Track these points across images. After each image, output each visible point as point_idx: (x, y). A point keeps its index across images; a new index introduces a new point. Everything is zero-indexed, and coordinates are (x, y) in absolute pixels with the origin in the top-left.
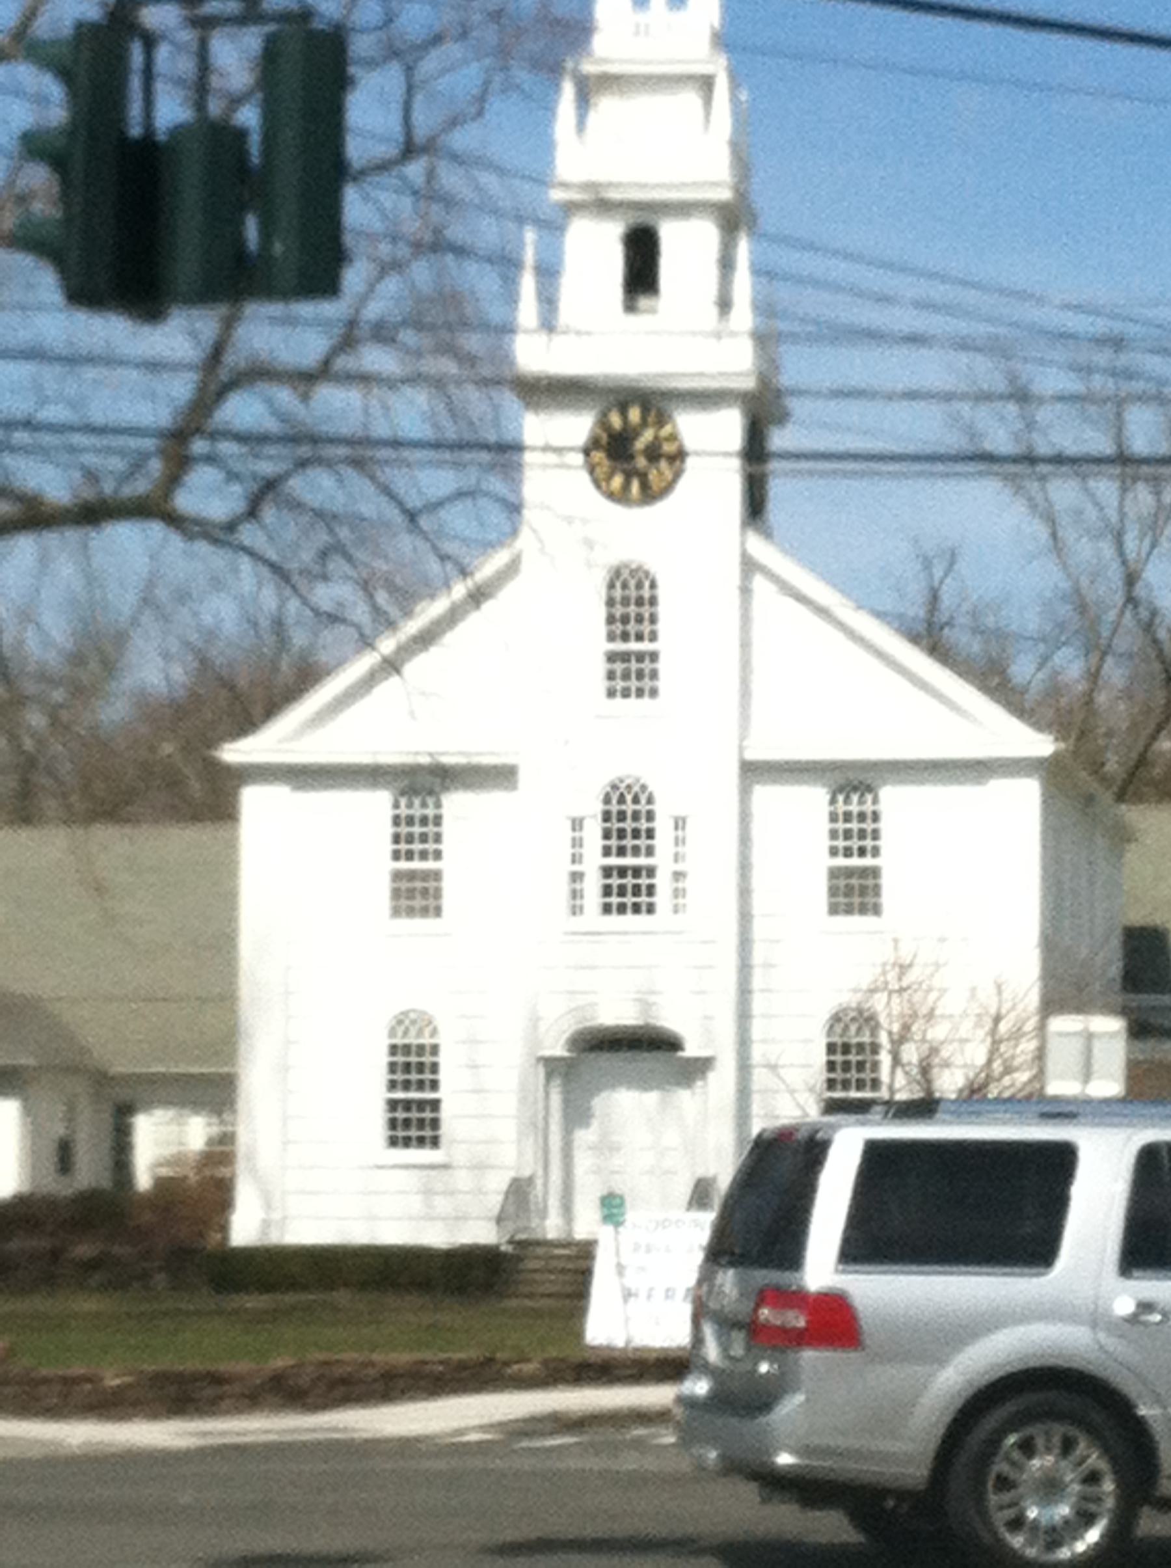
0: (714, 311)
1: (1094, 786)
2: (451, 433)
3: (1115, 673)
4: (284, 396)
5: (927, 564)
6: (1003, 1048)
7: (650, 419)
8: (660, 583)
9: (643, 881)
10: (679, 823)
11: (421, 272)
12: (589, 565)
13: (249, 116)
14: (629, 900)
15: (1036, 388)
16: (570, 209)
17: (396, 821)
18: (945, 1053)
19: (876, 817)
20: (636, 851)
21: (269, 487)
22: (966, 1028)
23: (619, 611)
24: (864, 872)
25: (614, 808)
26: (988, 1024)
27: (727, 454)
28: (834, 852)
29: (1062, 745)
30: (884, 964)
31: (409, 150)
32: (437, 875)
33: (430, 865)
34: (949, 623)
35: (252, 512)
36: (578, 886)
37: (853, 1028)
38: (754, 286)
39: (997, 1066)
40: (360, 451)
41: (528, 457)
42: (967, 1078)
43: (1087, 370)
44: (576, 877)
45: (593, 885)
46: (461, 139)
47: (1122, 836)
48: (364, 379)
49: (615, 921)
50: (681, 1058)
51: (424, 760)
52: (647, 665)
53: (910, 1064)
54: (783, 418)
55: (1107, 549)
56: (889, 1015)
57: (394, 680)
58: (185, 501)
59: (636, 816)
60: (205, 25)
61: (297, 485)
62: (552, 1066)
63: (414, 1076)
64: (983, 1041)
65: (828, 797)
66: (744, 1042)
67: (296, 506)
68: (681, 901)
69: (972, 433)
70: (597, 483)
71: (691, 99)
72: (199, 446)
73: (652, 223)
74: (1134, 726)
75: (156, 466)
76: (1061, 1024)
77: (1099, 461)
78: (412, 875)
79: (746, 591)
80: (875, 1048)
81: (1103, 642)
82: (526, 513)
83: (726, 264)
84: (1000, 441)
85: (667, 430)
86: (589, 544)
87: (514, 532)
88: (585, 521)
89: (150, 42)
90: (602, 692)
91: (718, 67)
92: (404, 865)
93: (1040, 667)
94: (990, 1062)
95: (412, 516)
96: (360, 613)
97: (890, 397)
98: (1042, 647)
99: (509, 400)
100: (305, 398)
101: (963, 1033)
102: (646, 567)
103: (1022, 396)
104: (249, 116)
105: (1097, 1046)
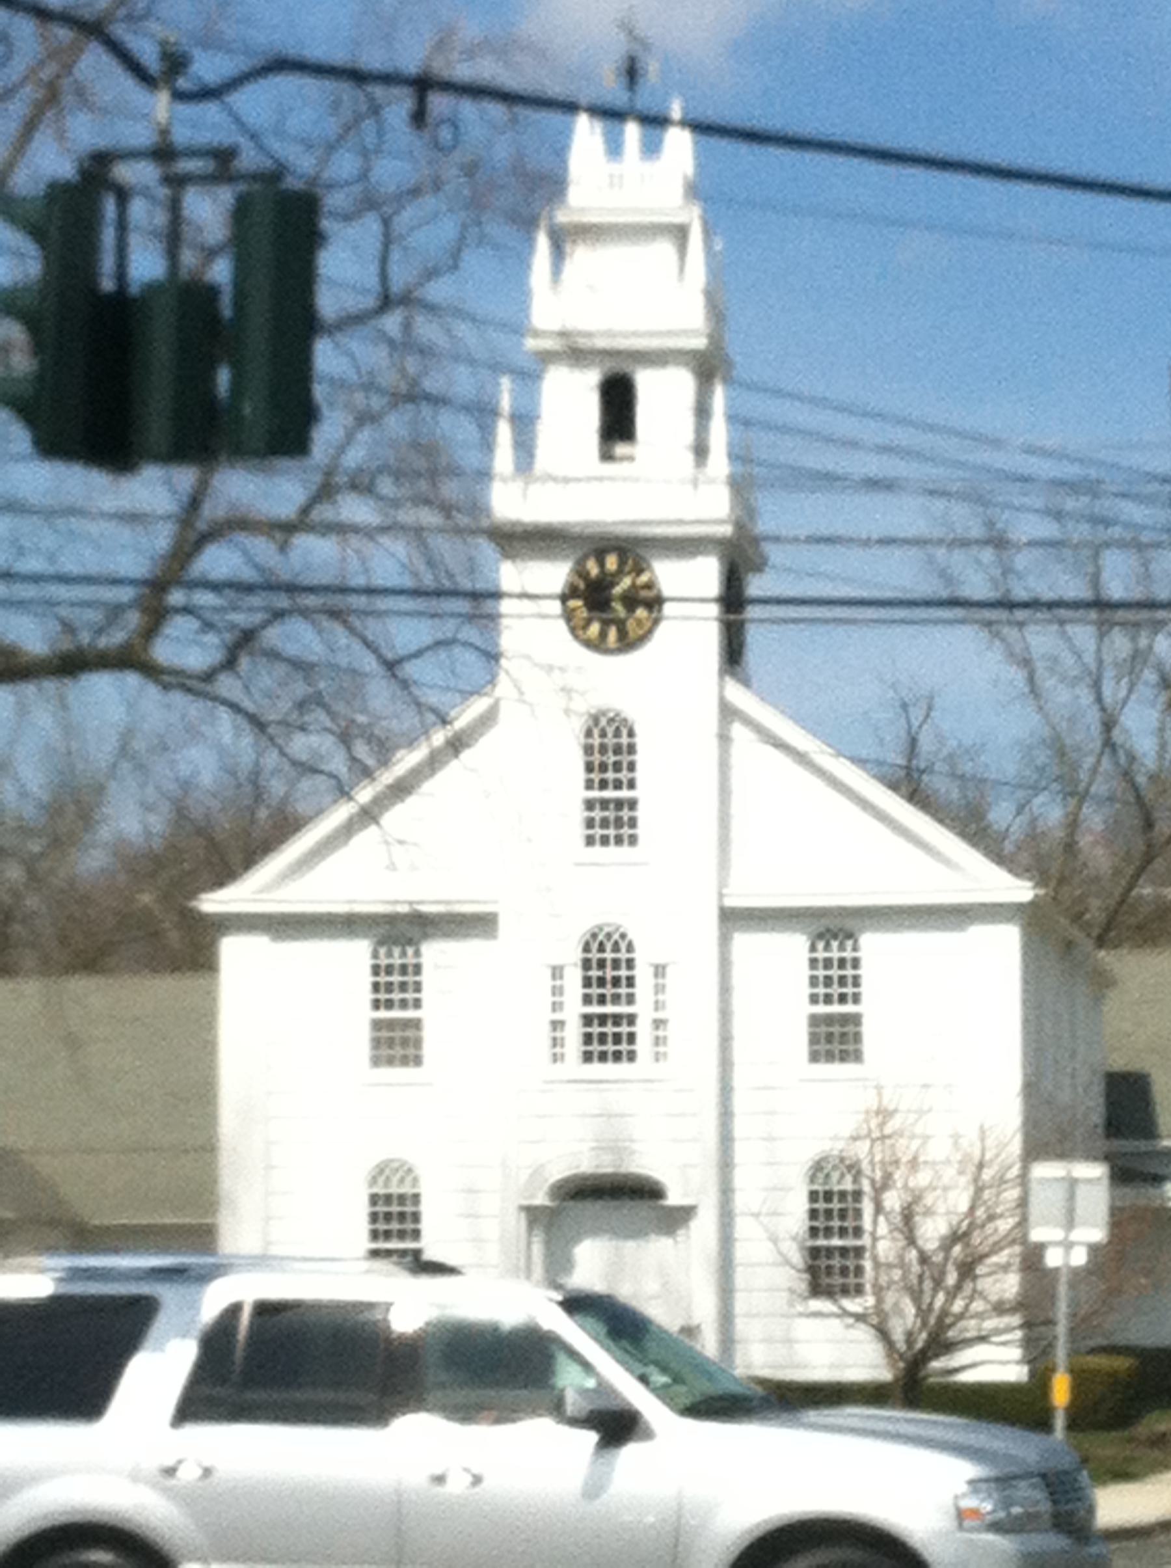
0: (690, 457)
1: (1076, 933)
2: (428, 581)
3: (1094, 819)
4: (262, 548)
5: (904, 706)
6: (986, 1194)
7: (627, 569)
8: (637, 729)
9: (624, 1029)
10: (659, 970)
11: (396, 424)
12: (567, 712)
13: (221, 272)
14: (610, 1048)
15: (1013, 536)
16: (546, 358)
17: (376, 970)
18: (929, 1200)
19: (856, 963)
20: (616, 999)
21: (246, 639)
22: (949, 1173)
23: (597, 758)
24: (845, 1019)
25: (595, 955)
26: (971, 1169)
27: (703, 600)
28: (814, 999)
29: (1041, 892)
30: (867, 1112)
31: (386, 302)
32: (416, 1024)
33: (410, 1014)
34: (929, 770)
35: (230, 663)
36: (558, 1034)
37: (835, 1176)
38: (728, 431)
39: (980, 1213)
40: (336, 601)
41: (506, 606)
42: (950, 1224)
43: (1058, 515)
44: (557, 1025)
45: (573, 1033)
46: (438, 291)
47: (1102, 982)
48: (340, 529)
49: (597, 1069)
50: (663, 1208)
51: (403, 909)
52: (625, 814)
53: (892, 1211)
54: (759, 566)
55: (1086, 697)
56: (872, 1163)
57: (373, 829)
58: (163, 652)
59: (616, 964)
60: (177, 182)
61: (273, 636)
62: (533, 1214)
63: (395, 1226)
64: (965, 1189)
65: (808, 945)
66: (726, 1191)
67: (274, 655)
68: (661, 1049)
69: (945, 575)
70: (573, 630)
71: (665, 248)
72: (176, 597)
73: (627, 370)
74: (1117, 872)
75: (134, 619)
76: (1045, 1170)
77: (1076, 605)
78: (391, 1024)
79: (724, 739)
80: (858, 1195)
81: (1082, 786)
82: (503, 662)
83: (702, 412)
84: (977, 586)
85: (644, 578)
86: (566, 691)
87: (492, 681)
88: (562, 669)
89: (123, 195)
90: (581, 841)
91: (692, 216)
92: (383, 1014)
93: (1019, 812)
94: (972, 1209)
95: (391, 666)
96: (338, 764)
97: (866, 543)
98: (1021, 794)
99: (486, 549)
100: (283, 548)
101: (946, 1180)
102: (623, 715)
103: (999, 542)
104: (221, 272)
105: (1082, 1191)
